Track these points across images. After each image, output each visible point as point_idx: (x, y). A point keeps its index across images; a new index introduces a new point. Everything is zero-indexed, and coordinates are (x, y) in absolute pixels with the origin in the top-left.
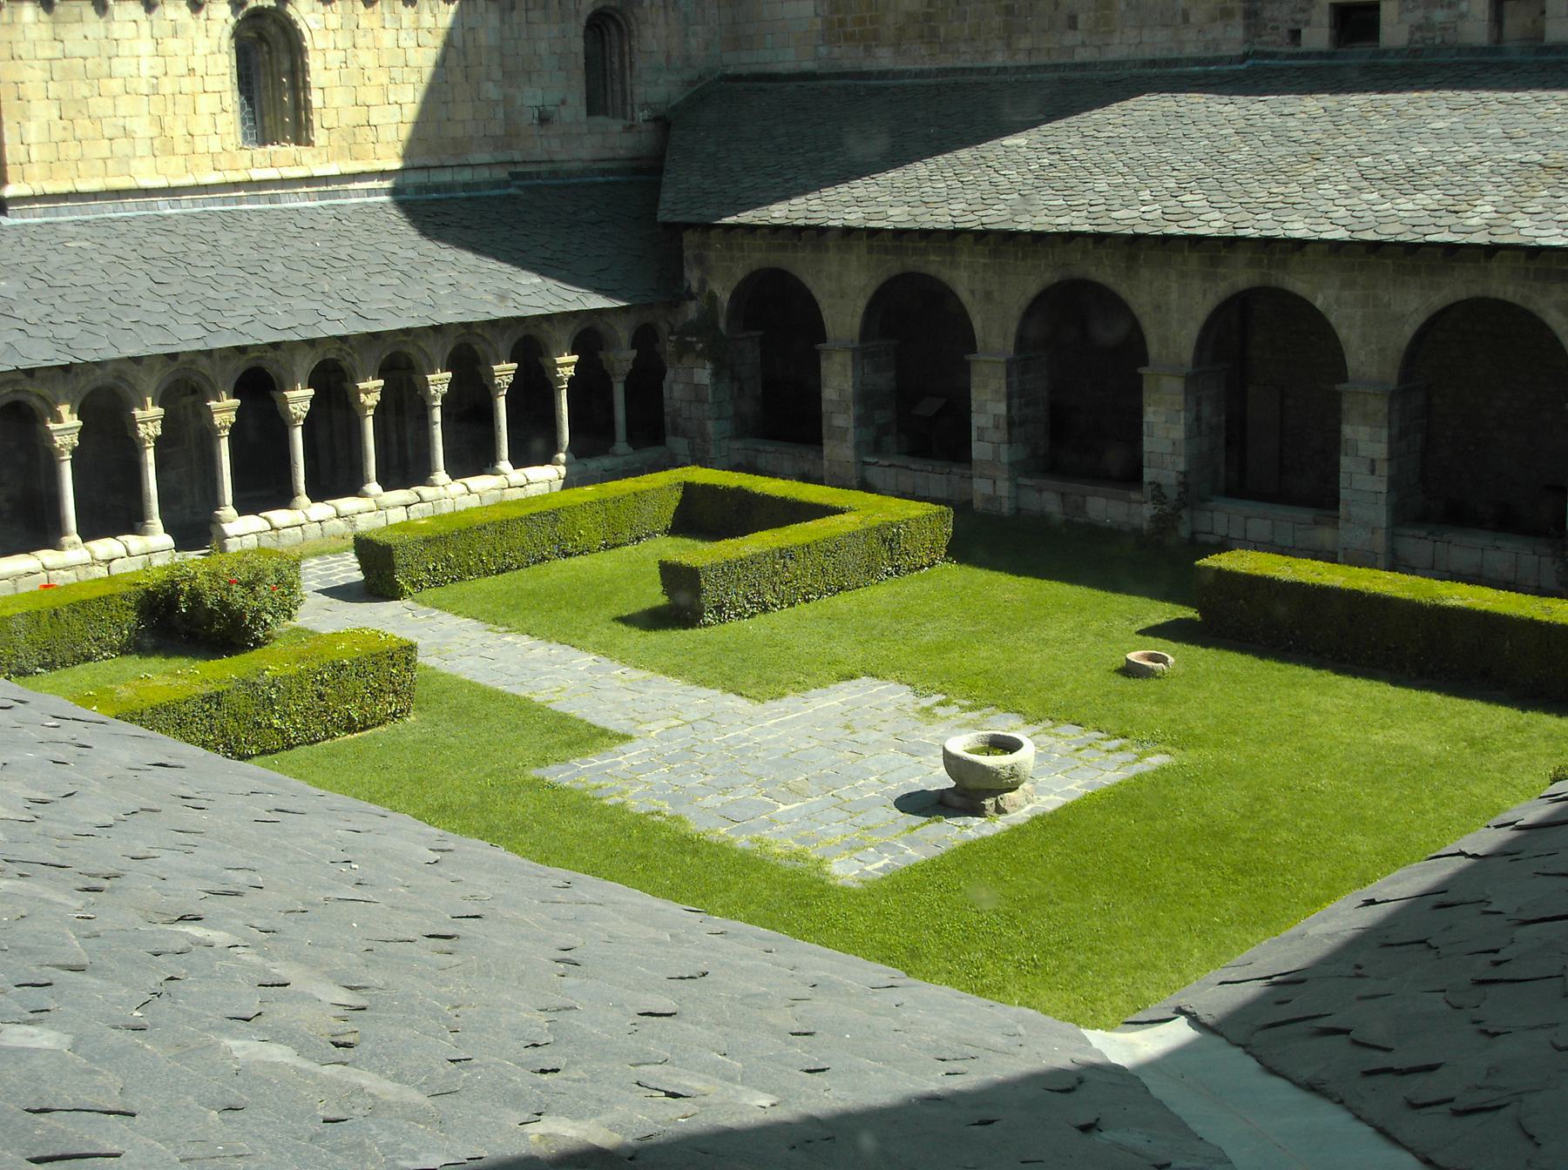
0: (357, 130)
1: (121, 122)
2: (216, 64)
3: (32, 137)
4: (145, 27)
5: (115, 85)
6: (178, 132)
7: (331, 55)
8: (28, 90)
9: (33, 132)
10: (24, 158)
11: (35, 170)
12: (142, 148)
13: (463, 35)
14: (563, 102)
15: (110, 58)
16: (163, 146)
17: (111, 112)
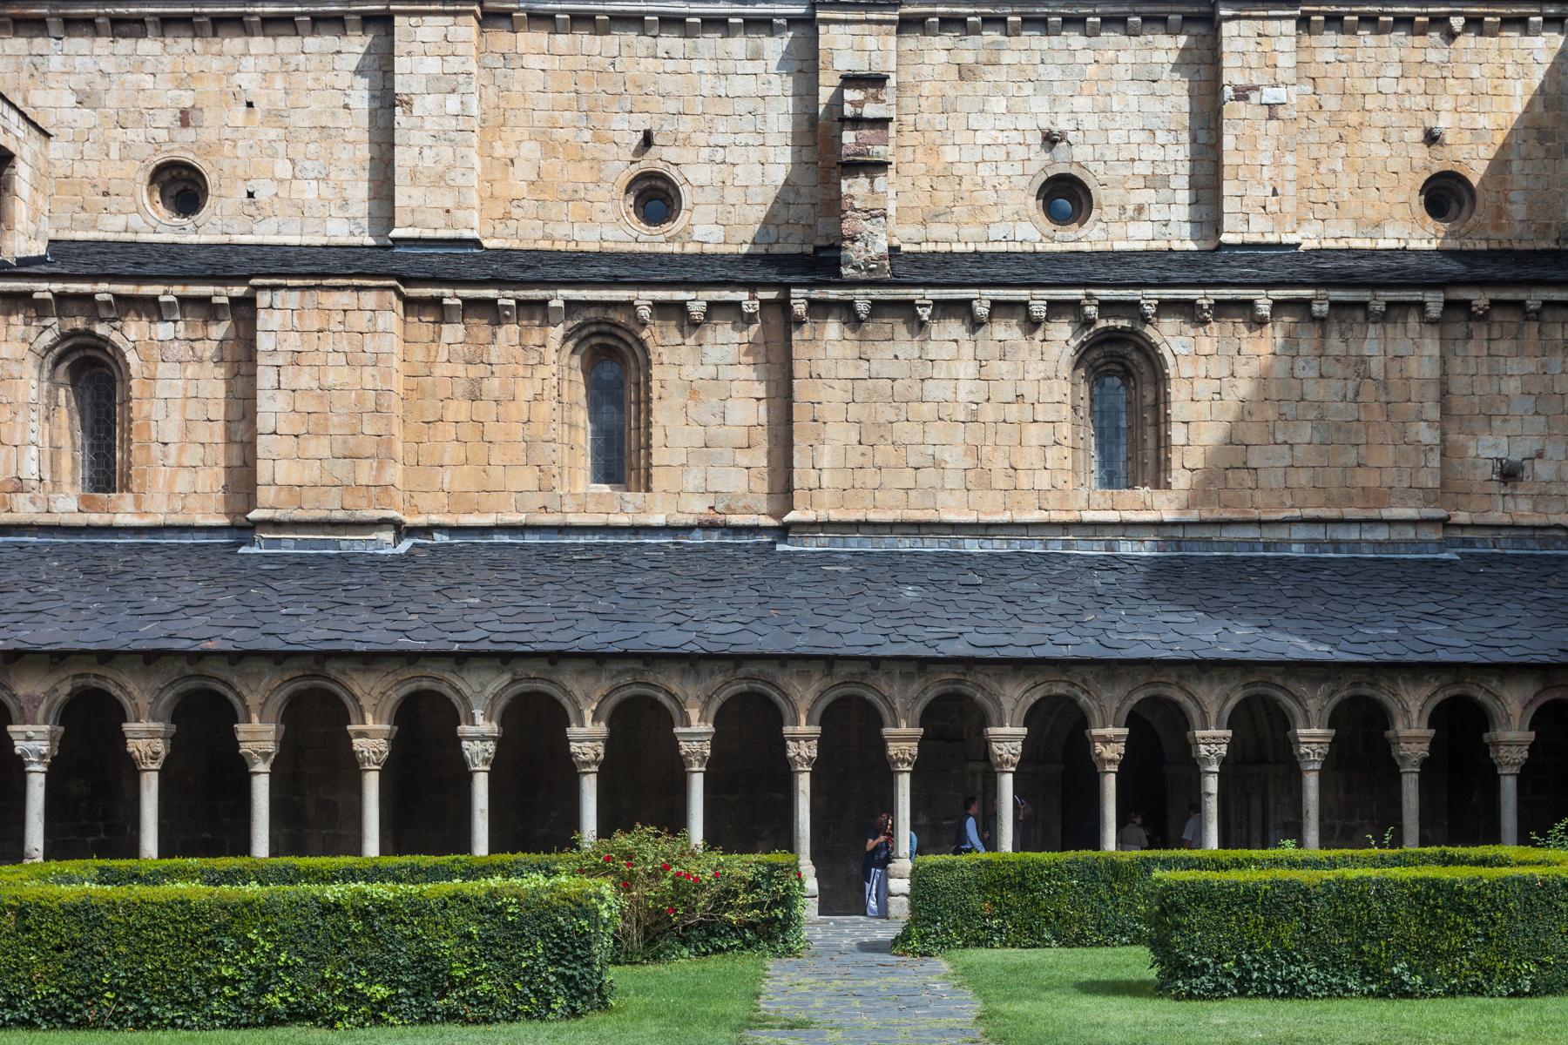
0: (1230, 473)
1: (930, 450)
2: (1051, 391)
3: (825, 462)
4: (967, 349)
5: (927, 410)
6: (998, 463)
7: (1200, 385)
8: (825, 412)
9: (826, 457)
10: (813, 483)
11: (826, 497)
12: (953, 480)
13: (1385, 365)
14: (1540, 455)
15: (923, 380)
16: (978, 477)
17: (918, 439)
